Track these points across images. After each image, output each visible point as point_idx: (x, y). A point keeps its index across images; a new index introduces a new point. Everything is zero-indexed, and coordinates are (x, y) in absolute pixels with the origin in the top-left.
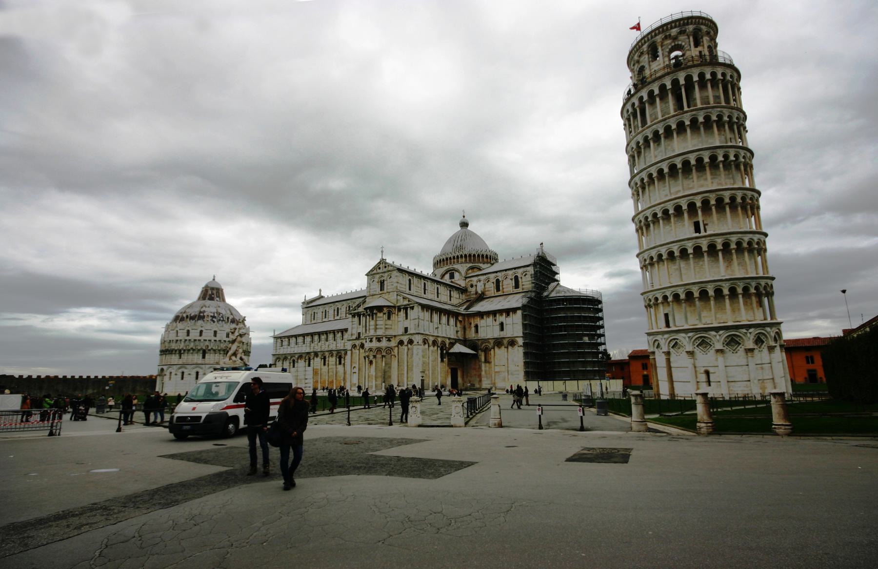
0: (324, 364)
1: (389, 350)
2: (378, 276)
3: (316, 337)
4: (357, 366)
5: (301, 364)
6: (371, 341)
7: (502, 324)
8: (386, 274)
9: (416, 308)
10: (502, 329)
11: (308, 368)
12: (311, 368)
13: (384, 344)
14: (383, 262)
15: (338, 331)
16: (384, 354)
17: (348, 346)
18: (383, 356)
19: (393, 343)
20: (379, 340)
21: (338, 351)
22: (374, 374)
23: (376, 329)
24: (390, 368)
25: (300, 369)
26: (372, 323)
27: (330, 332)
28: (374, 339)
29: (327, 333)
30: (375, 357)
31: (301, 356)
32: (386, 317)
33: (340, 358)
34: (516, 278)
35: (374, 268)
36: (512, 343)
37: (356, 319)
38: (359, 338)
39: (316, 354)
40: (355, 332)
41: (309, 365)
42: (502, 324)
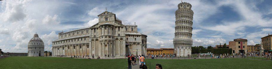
0: (69, 49)
1: (113, 41)
3: (65, 41)
5: (61, 49)
7: (135, 39)
9: (123, 28)
11: (63, 50)
12: (64, 50)
13: (111, 39)
20: (110, 37)
21: (74, 45)
23: (108, 33)
25: (61, 50)
29: (69, 40)
30: (108, 43)
31: (61, 47)
33: (74, 47)
34: (132, 29)
37: (93, 30)
39: (66, 46)
41: (63, 49)
42: (135, 39)
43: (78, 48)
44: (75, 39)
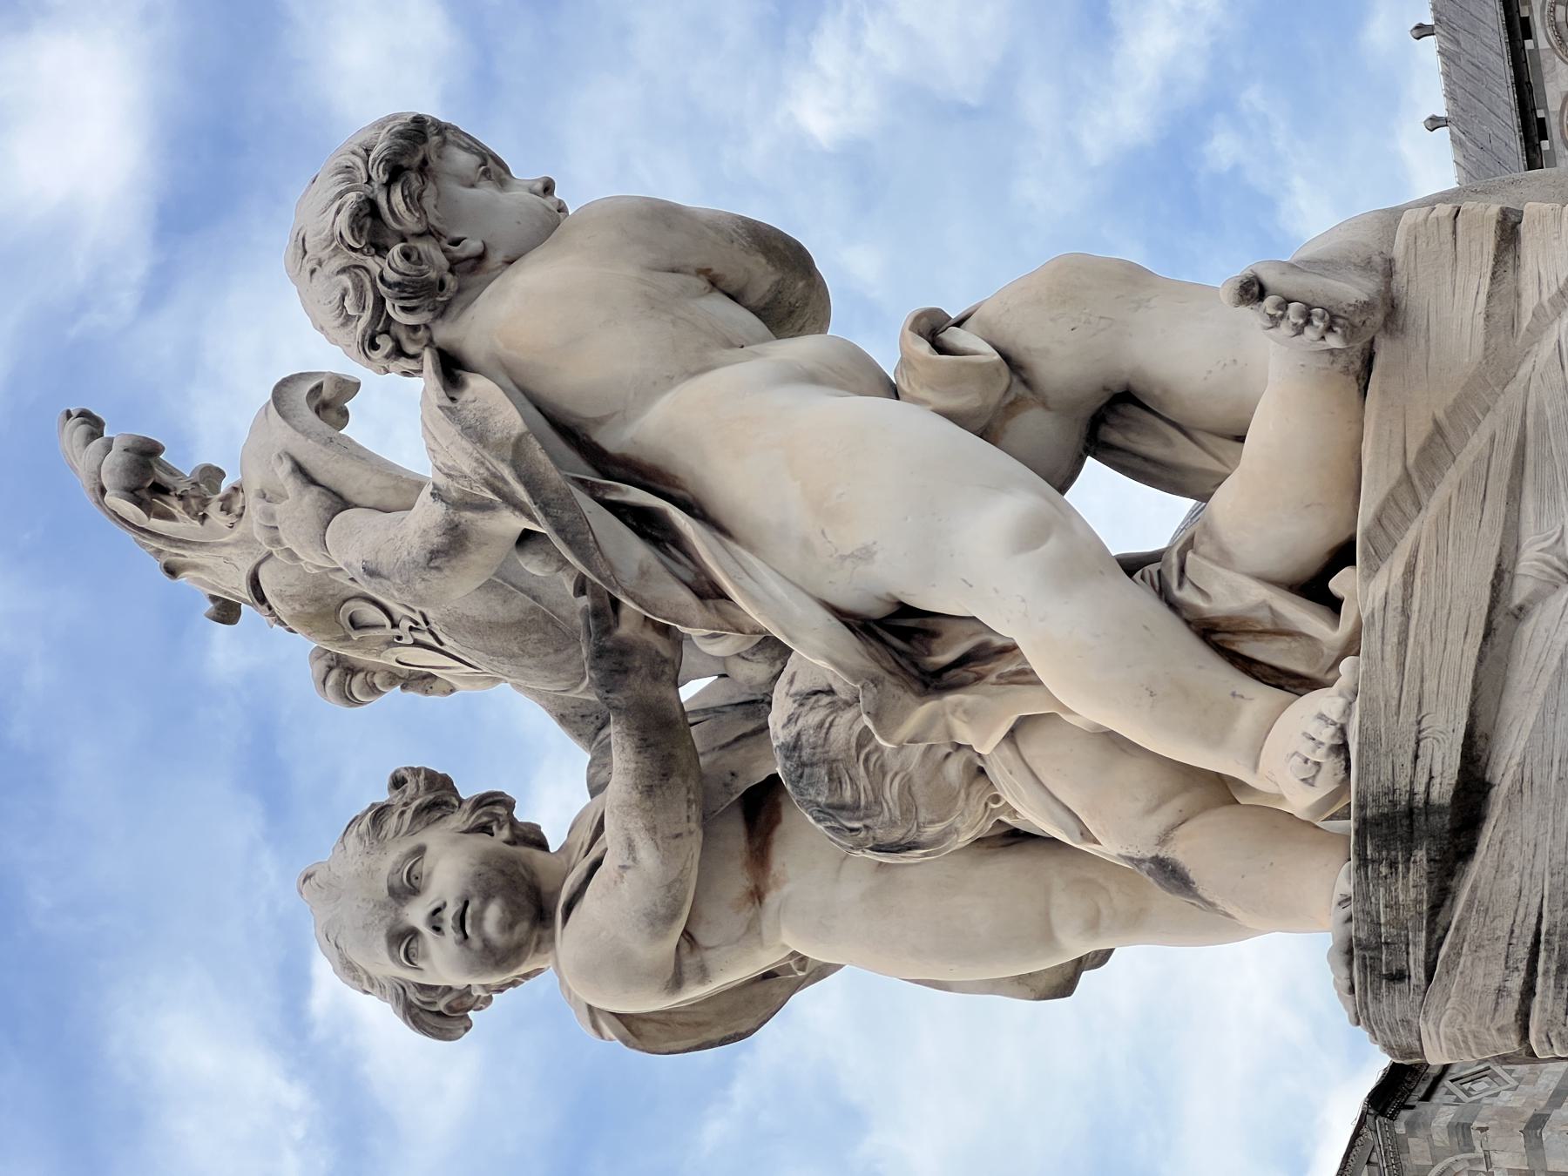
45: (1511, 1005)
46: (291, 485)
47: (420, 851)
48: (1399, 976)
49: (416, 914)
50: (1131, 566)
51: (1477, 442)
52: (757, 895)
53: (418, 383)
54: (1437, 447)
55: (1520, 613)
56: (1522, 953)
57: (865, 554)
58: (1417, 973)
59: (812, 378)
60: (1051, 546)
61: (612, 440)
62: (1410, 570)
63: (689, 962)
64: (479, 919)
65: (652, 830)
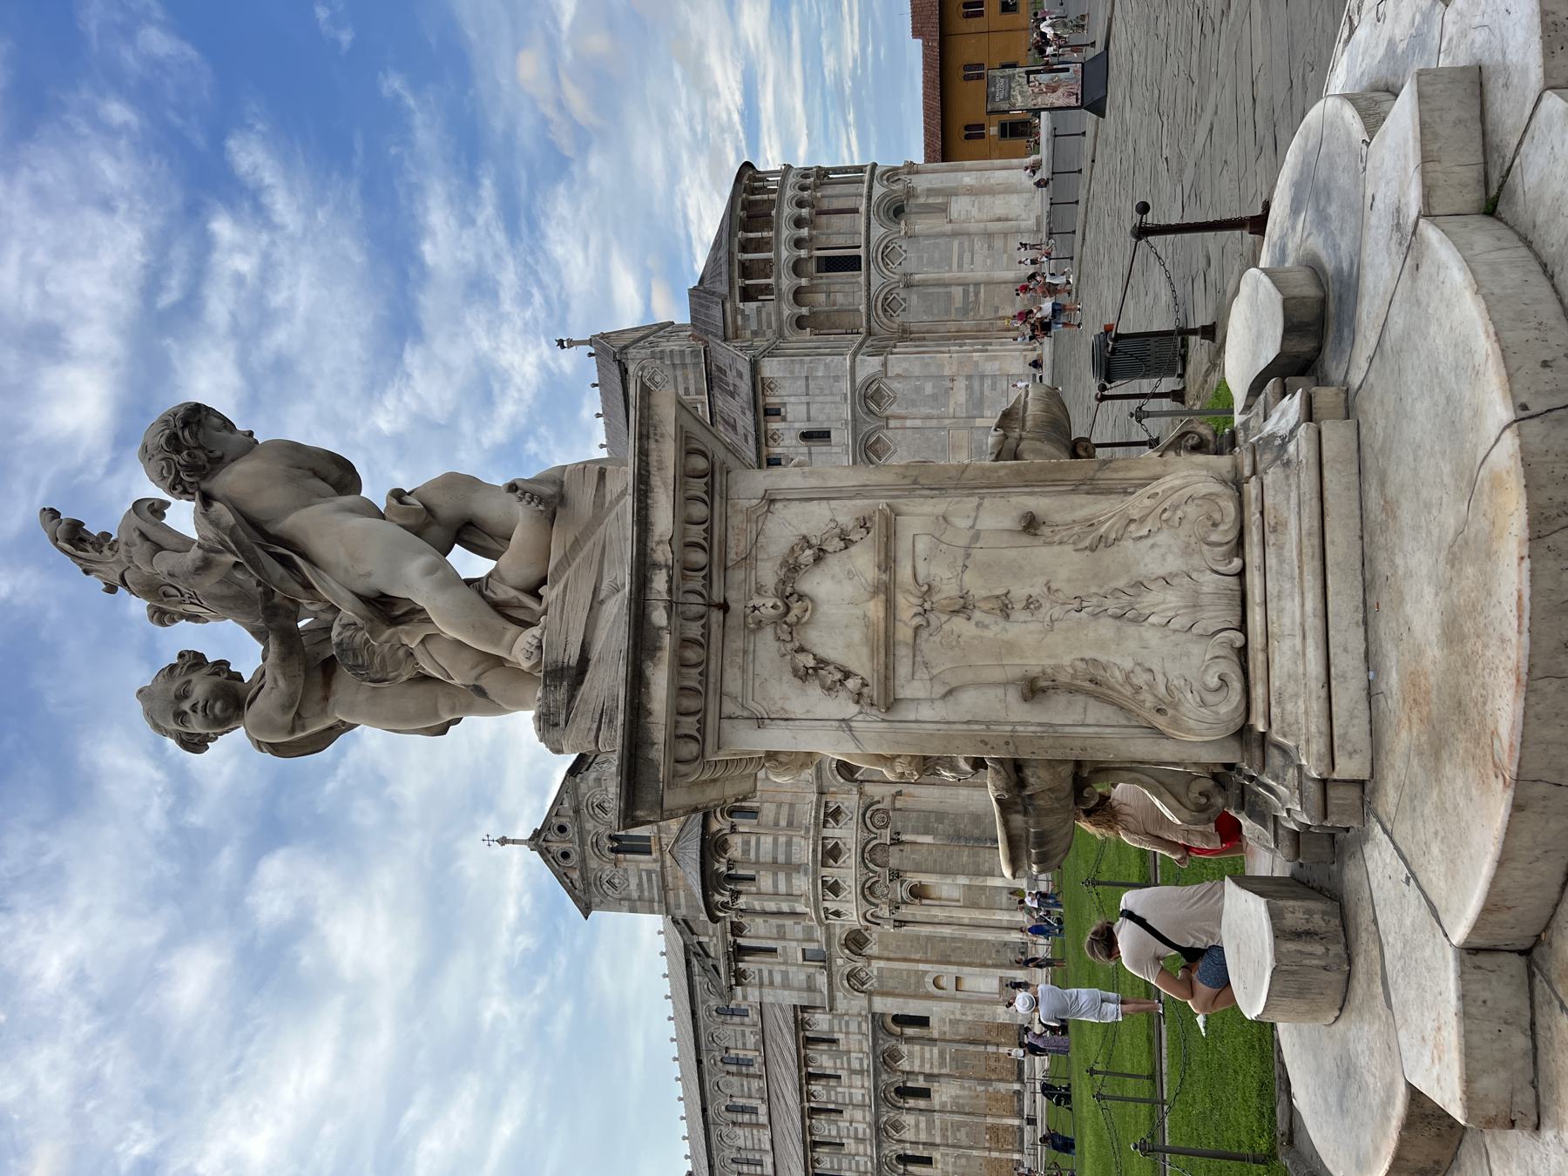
0: (928, 1161)
1: (871, 814)
2: (593, 863)
4: (933, 969)
6: (835, 888)
7: (807, 436)
8: (589, 825)
10: (823, 435)
13: (847, 834)
14: (538, 840)
15: (805, 1095)
16: (886, 836)
17: (851, 1003)
18: (896, 842)
19: (849, 801)
20: (832, 854)
22: (963, 880)
23: (791, 868)
24: (940, 816)
26: (765, 882)
27: (807, 1130)
28: (830, 873)
29: (811, 1145)
30: (896, 875)
32: (744, 825)
33: (904, 1092)
35: (562, 877)
36: (870, 397)
38: (823, 960)
40: (799, 976)
43: (916, 1059)
44: (811, 1077)
45: (593, 734)
46: (138, 541)
47: (189, 682)
48: (557, 725)
49: (186, 706)
50: (469, 582)
51: (589, 545)
52: (326, 699)
53: (193, 504)
54: (577, 544)
55: (602, 602)
56: (597, 716)
57: (369, 575)
58: (562, 723)
59: (352, 510)
60: (439, 574)
61: (273, 529)
62: (566, 587)
63: (299, 723)
64: (212, 707)
65: (284, 674)
